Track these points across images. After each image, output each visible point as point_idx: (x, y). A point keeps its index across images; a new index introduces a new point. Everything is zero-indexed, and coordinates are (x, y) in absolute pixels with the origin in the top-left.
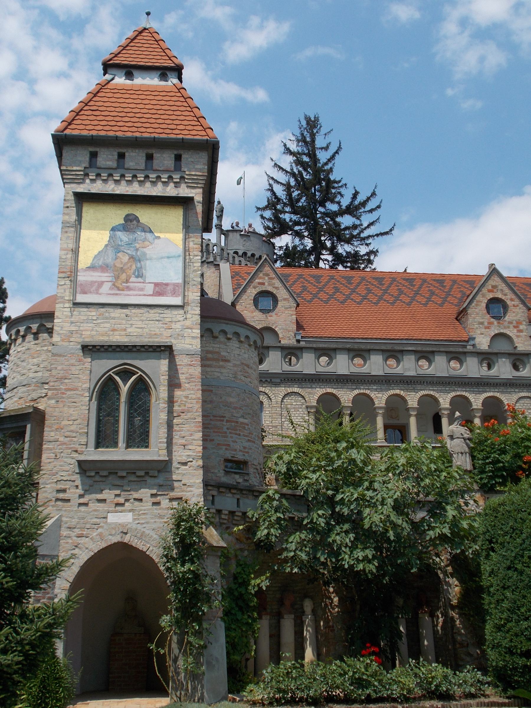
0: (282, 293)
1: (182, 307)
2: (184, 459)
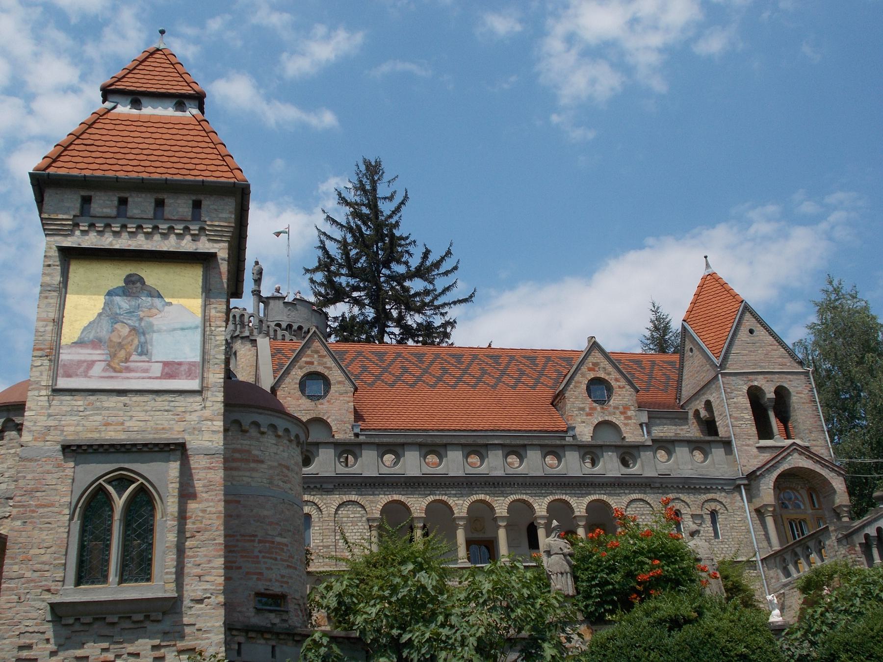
1: (199, 392)
2: (199, 595)
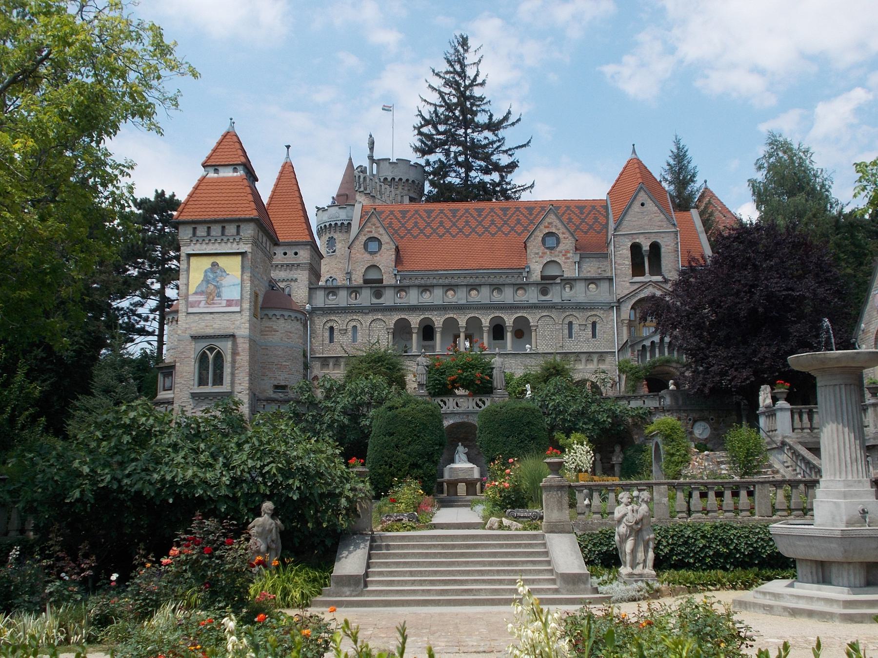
0: (385, 238)
2: (239, 391)
